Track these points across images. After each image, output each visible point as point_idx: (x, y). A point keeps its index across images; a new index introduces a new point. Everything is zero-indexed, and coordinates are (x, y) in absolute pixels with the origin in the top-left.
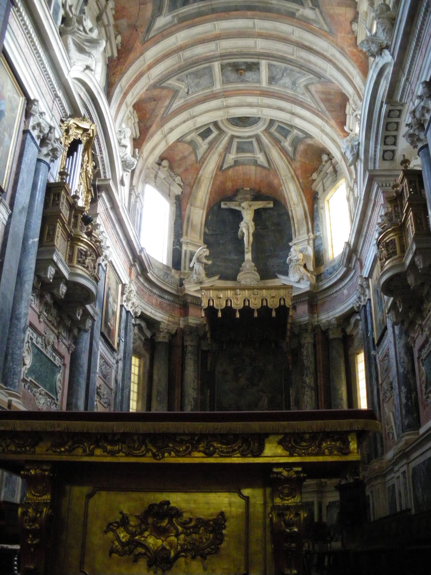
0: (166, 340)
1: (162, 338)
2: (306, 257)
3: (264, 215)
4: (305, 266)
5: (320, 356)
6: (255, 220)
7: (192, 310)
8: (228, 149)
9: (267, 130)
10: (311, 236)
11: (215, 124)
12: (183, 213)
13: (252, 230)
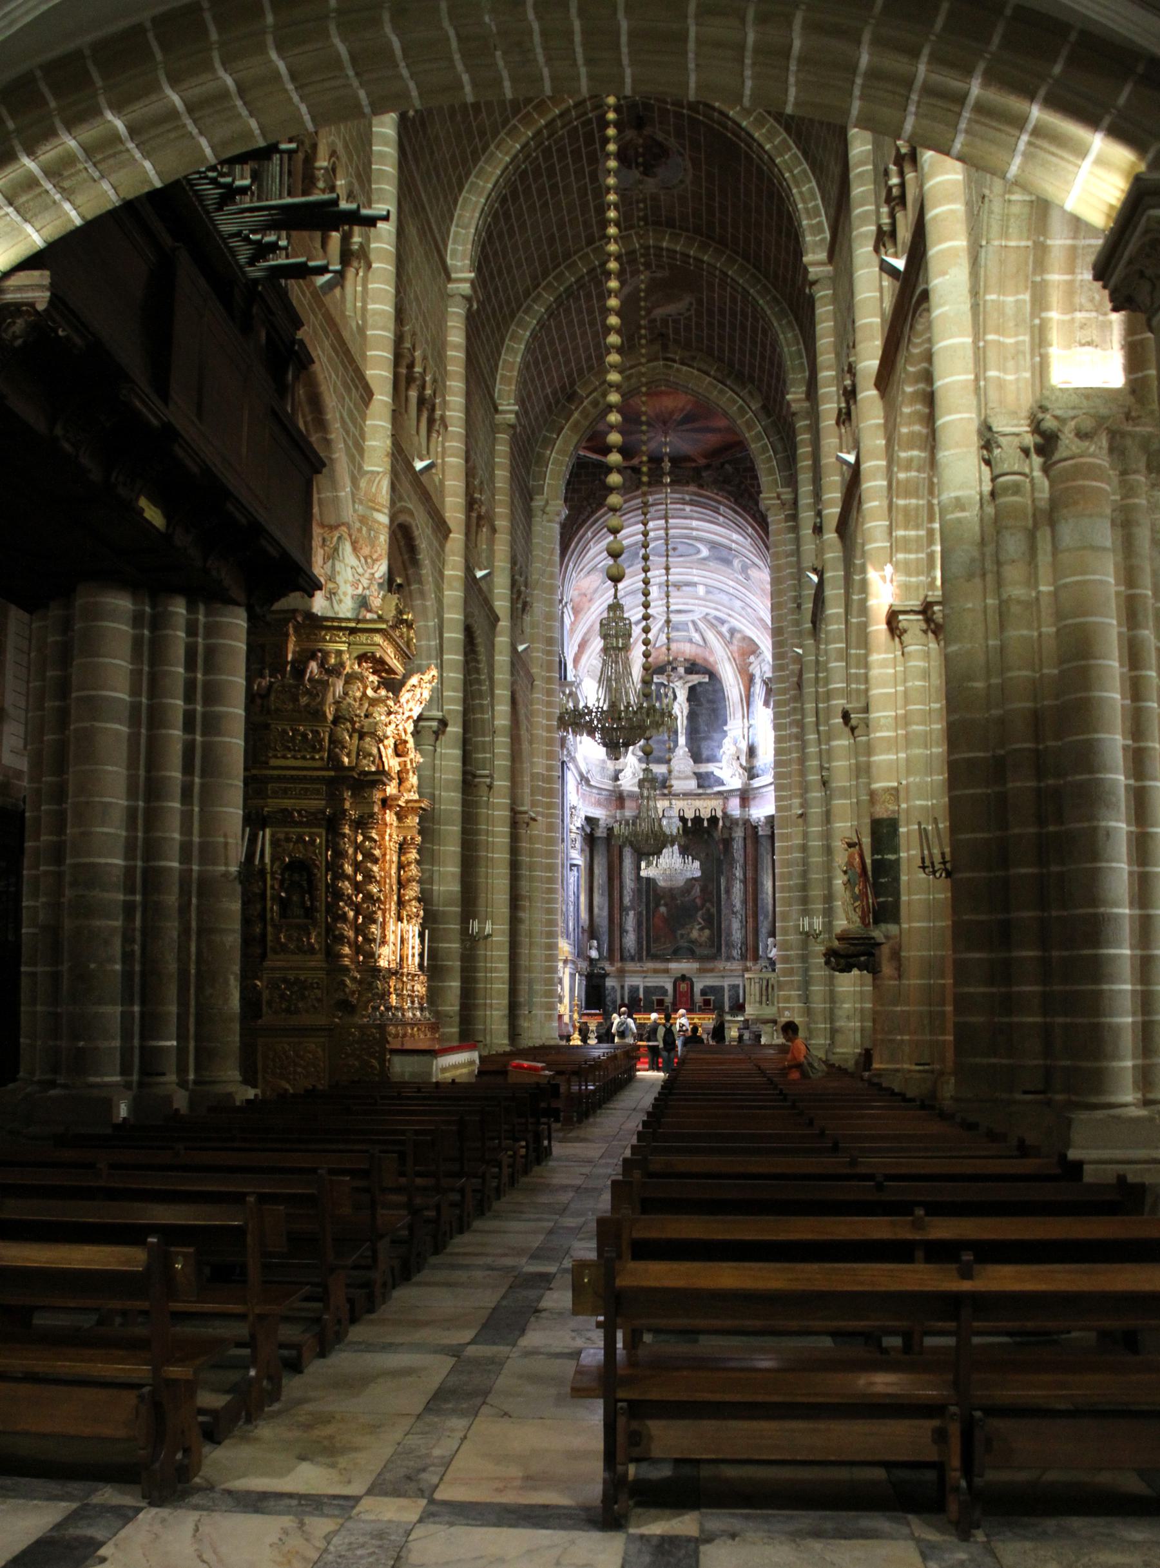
0: (605, 835)
1: (601, 832)
2: (738, 750)
3: (699, 689)
5: (750, 850)
6: (689, 700)
7: (628, 803)
10: (746, 725)
13: (686, 712)
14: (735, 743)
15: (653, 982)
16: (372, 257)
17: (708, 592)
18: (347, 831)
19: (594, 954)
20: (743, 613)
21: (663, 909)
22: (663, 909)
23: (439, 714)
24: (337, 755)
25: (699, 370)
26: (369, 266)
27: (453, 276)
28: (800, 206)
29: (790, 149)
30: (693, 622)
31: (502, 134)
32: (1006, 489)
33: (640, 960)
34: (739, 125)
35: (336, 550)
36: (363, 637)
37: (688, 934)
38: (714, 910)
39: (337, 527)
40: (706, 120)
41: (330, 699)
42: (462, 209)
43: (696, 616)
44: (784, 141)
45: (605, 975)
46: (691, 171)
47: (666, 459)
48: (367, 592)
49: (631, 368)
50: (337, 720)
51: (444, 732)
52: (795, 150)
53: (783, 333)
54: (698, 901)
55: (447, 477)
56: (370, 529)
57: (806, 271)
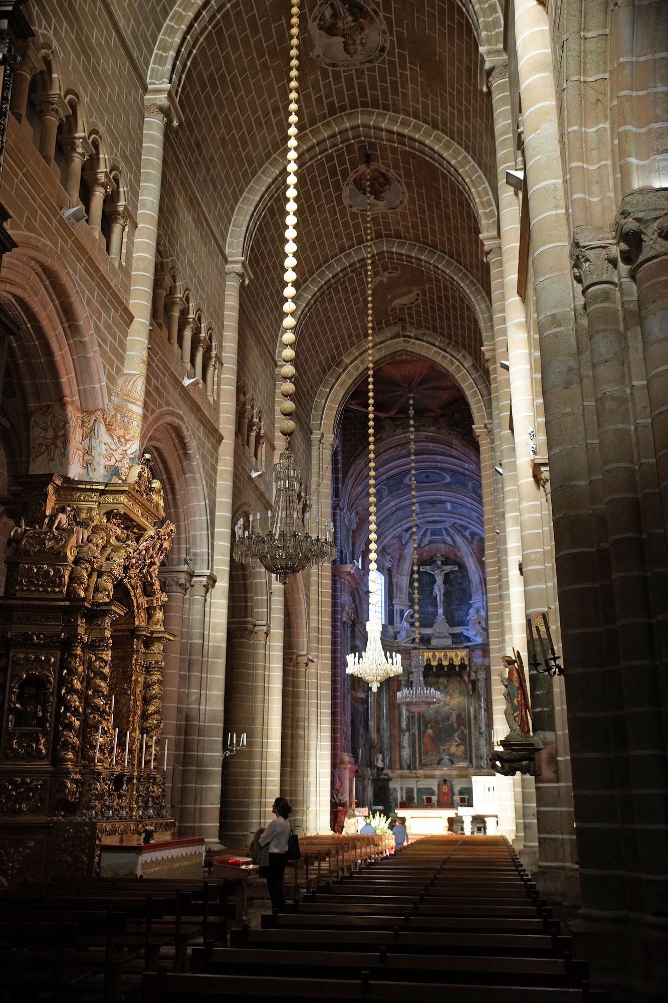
3: (452, 576)
4: (480, 622)
6: (444, 583)
8: (424, 535)
9: (452, 526)
11: (417, 525)
12: (393, 580)
13: (442, 592)
14: (478, 611)
15: (424, 784)
16: (138, 220)
17: (453, 508)
18: (79, 652)
19: (380, 764)
20: (478, 521)
21: (430, 731)
22: (430, 731)
23: (208, 572)
24: (74, 588)
25: (428, 343)
26: (135, 226)
27: (229, 259)
28: (477, 200)
29: (469, 162)
30: (445, 529)
31: (266, 164)
32: (596, 298)
33: (415, 768)
34: (433, 150)
35: (92, 430)
36: (110, 498)
37: (448, 749)
38: (466, 732)
39: (93, 412)
40: (411, 150)
41: (73, 541)
42: (237, 214)
43: (447, 525)
44: (465, 156)
45: (389, 780)
46: (407, 194)
47: (411, 408)
48: (120, 464)
49: (381, 343)
50: (77, 561)
51: (213, 586)
52: (473, 162)
53: (478, 305)
54: (455, 725)
55: (221, 400)
56: (124, 416)
57: (483, 245)
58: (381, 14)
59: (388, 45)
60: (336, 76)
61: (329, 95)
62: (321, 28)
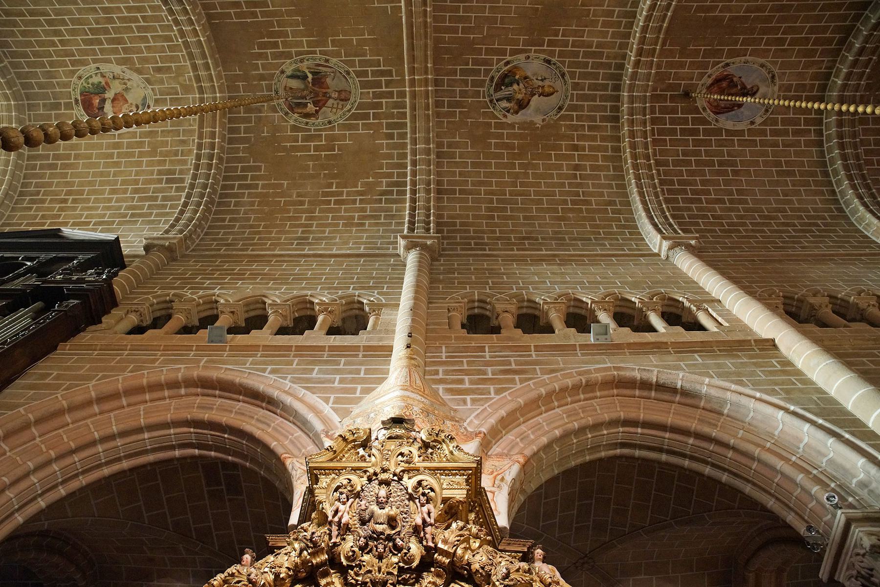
58: (508, 58)
59: (543, 56)
60: (573, 108)
61: (593, 119)
62: (517, 112)
